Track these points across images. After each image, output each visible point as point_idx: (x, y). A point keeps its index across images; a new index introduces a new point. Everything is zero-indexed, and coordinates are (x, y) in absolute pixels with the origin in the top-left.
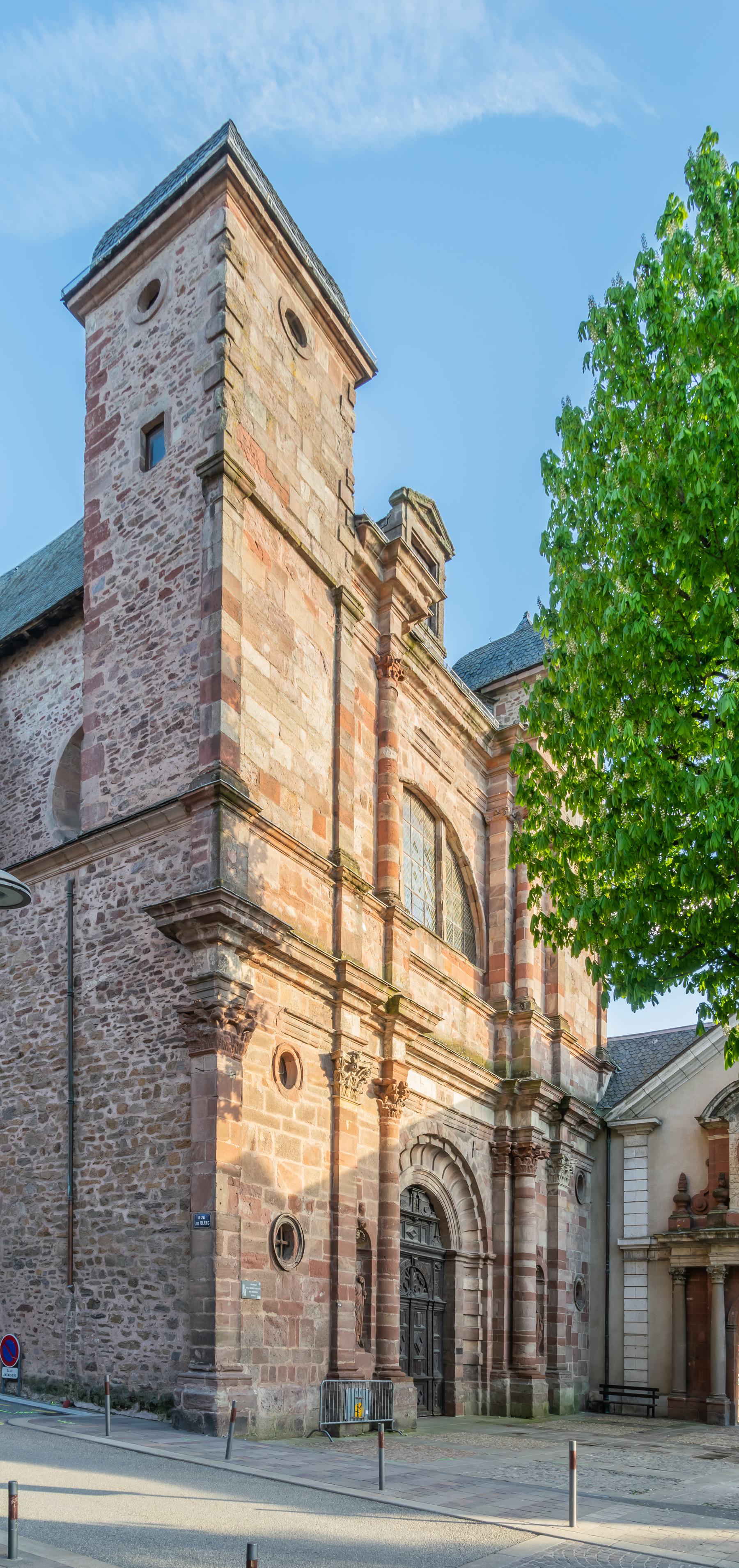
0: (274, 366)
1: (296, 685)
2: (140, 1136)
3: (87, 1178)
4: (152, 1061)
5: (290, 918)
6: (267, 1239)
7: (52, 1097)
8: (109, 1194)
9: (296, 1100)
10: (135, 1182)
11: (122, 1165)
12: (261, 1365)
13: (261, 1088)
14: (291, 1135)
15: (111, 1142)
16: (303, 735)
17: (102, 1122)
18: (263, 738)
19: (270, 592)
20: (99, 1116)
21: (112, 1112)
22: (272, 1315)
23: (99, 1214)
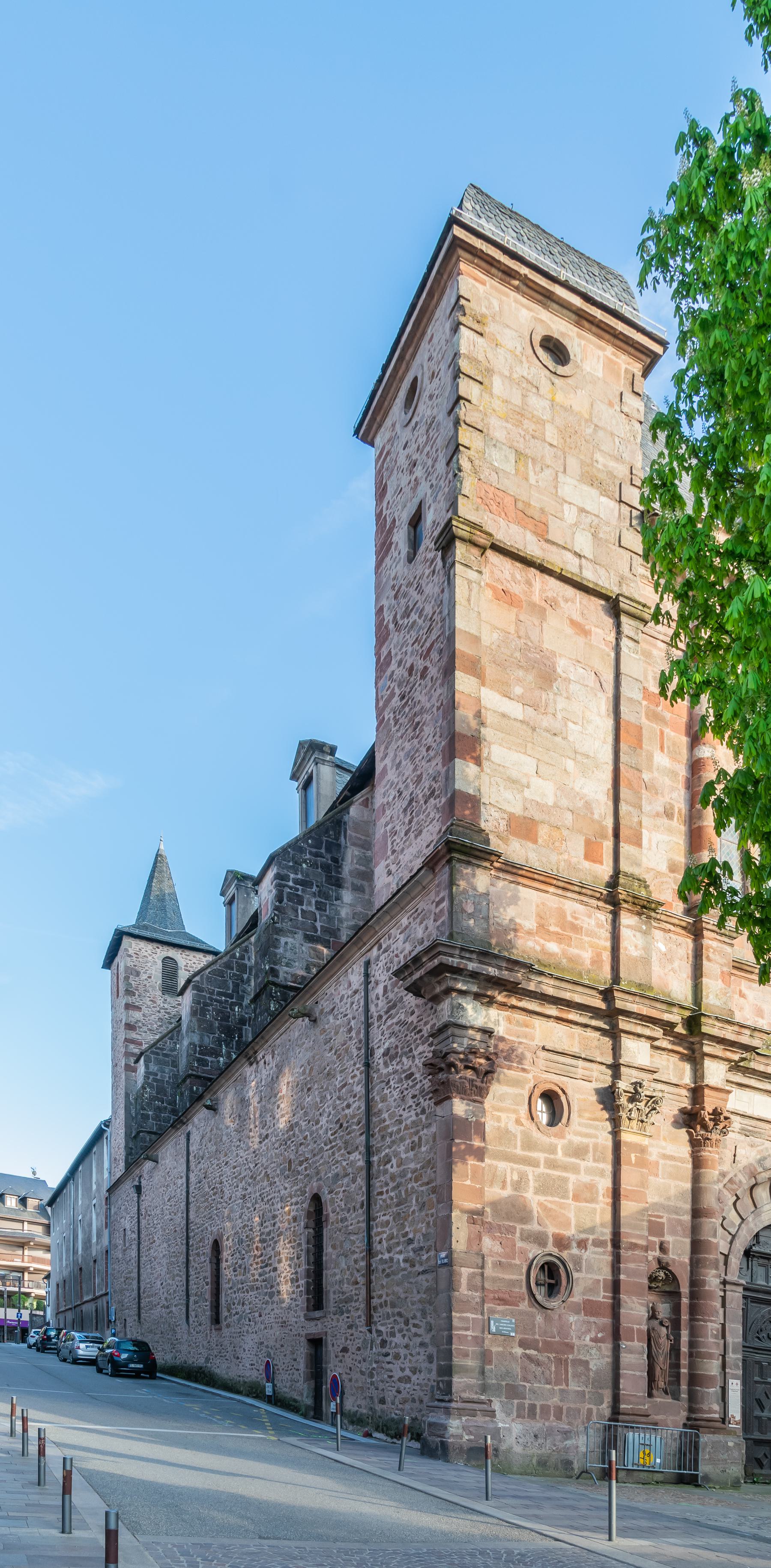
0: (524, 403)
1: (559, 716)
2: (410, 1186)
3: (379, 1229)
4: (417, 1115)
5: (551, 955)
6: (524, 1277)
7: (358, 1158)
8: (391, 1242)
9: (563, 1137)
10: (407, 1229)
11: (399, 1214)
12: (516, 1401)
13: (512, 1127)
14: (556, 1173)
15: (392, 1194)
16: (570, 765)
17: (388, 1176)
18: (514, 782)
19: (522, 633)
20: (386, 1172)
21: (393, 1168)
22: (532, 1352)
23: (386, 1262)
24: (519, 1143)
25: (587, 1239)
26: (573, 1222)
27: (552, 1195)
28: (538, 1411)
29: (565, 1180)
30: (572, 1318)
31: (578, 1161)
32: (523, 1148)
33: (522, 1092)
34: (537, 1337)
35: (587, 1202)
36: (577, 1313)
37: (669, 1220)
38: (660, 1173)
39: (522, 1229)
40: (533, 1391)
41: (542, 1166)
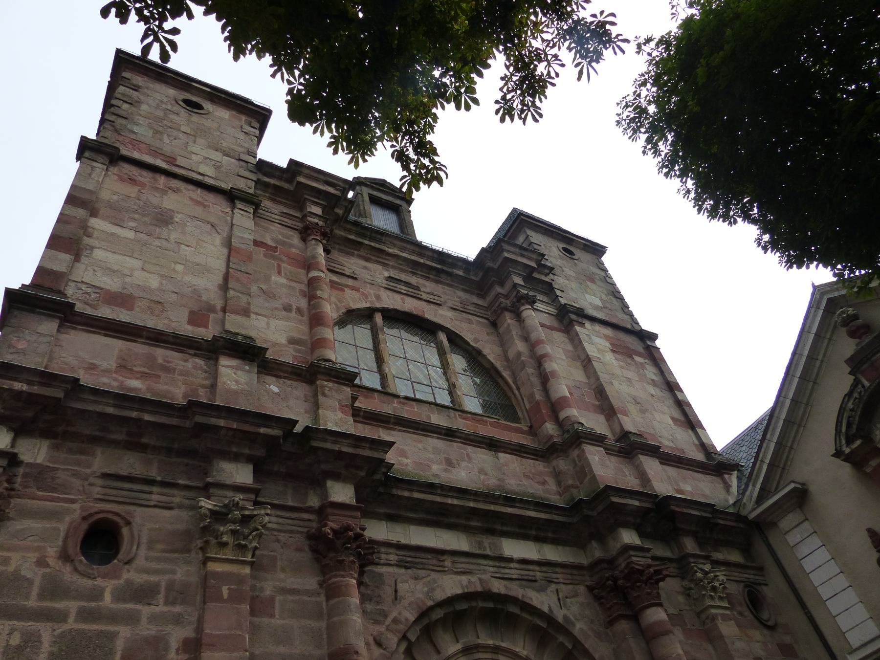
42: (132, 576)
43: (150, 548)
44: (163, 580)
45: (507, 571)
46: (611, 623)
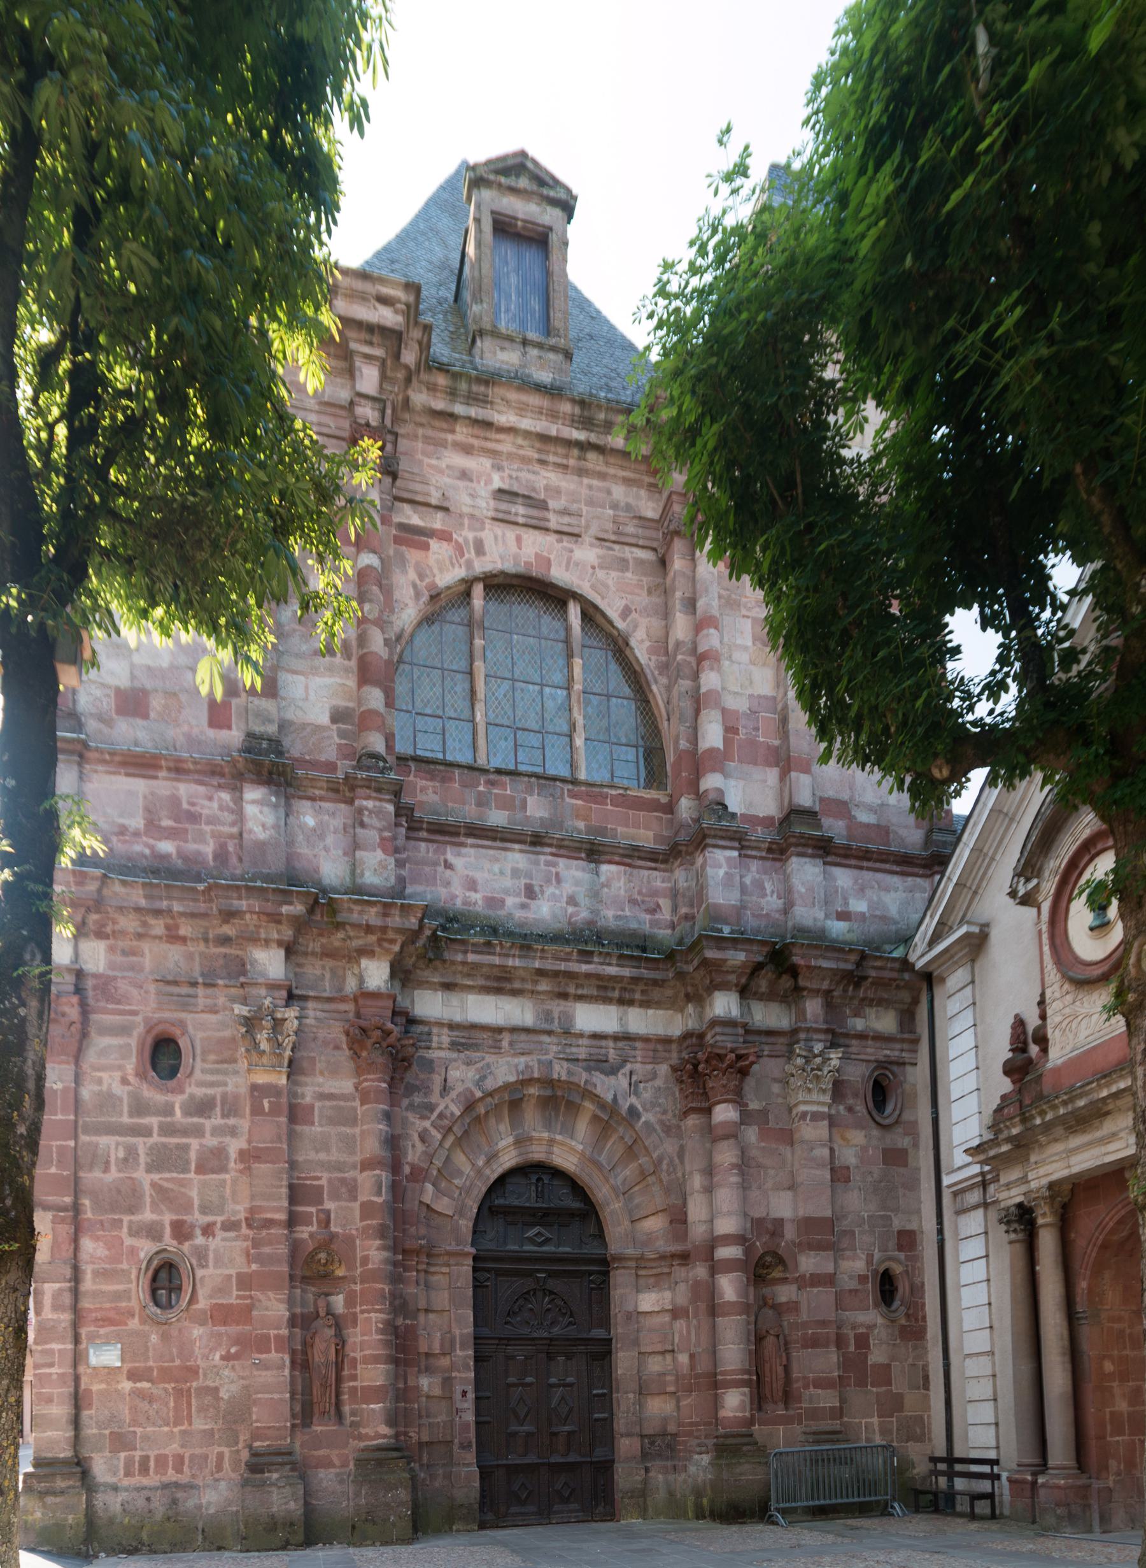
12: (123, 1455)
22: (145, 1385)
24: (126, 1109)
25: (214, 1223)
26: (196, 1203)
27: (170, 1171)
28: (152, 1464)
29: (186, 1148)
30: (197, 1332)
31: (202, 1120)
32: (131, 1115)
33: (129, 1041)
34: (151, 1363)
35: (213, 1172)
36: (203, 1324)
37: (330, 1181)
38: (316, 1119)
39: (130, 1222)
40: (146, 1438)
41: (155, 1135)
42: (194, 1090)
43: (204, 1061)
44: (216, 1091)
45: (574, 1050)
46: (685, 1114)
